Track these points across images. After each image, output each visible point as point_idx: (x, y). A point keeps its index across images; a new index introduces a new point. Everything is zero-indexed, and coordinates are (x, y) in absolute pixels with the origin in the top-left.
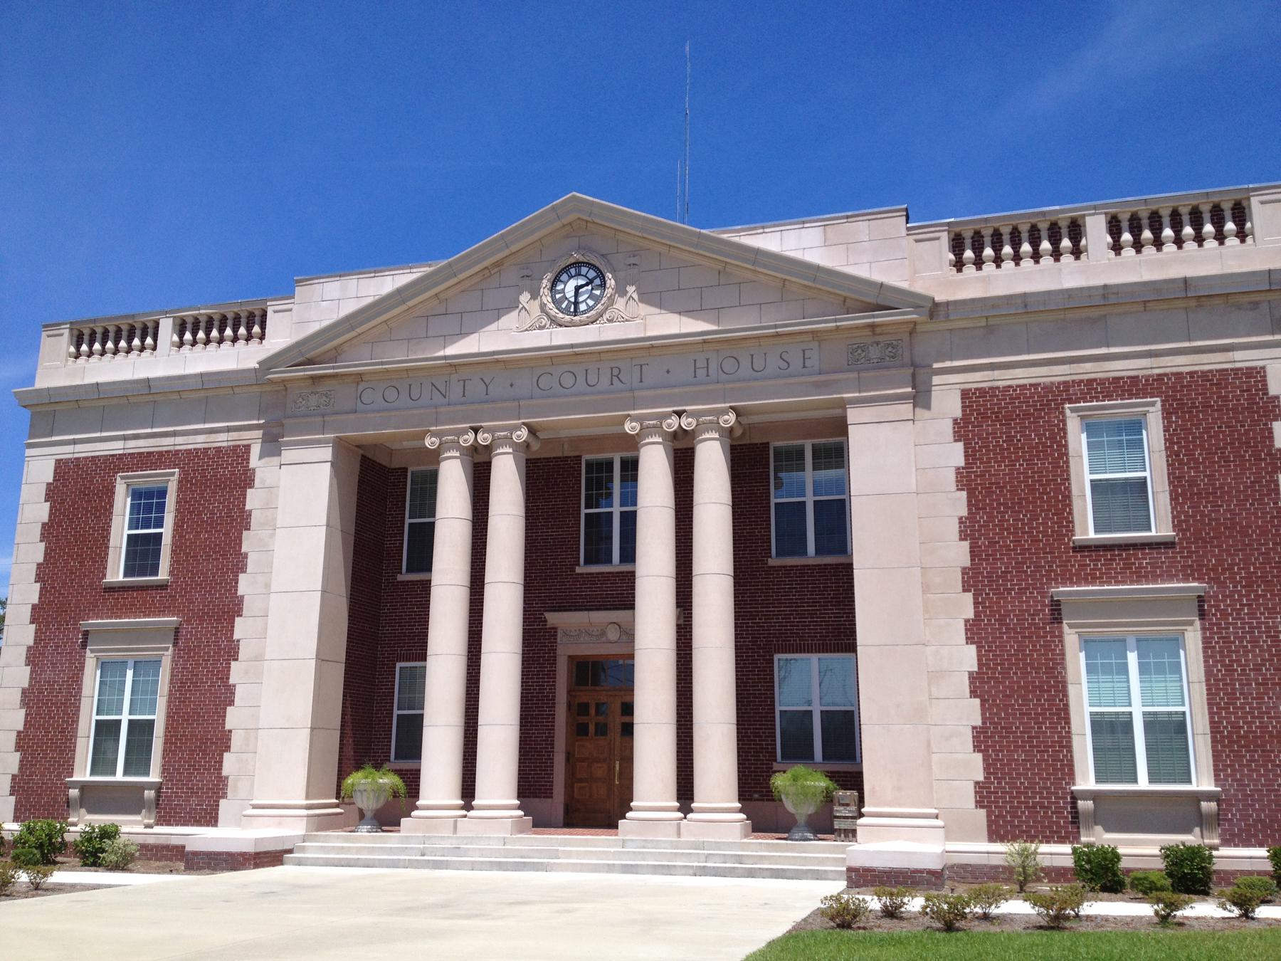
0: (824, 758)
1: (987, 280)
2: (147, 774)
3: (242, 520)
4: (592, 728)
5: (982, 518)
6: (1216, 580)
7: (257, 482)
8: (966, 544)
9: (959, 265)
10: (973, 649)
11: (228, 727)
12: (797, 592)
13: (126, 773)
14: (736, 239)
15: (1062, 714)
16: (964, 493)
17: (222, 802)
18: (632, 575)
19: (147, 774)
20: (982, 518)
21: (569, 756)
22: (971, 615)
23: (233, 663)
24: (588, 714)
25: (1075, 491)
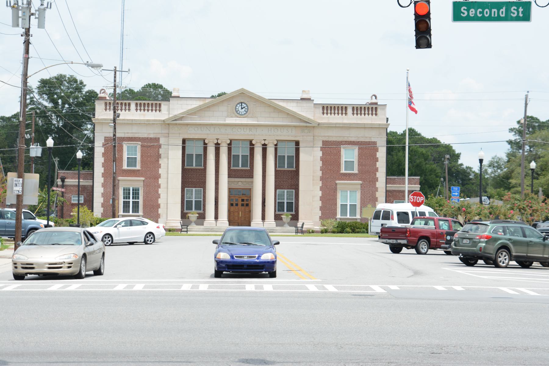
1: (329, 118)
2: (138, 212)
3: (159, 156)
5: (324, 167)
9: (323, 113)
12: (288, 178)
13: (133, 212)
15: (336, 204)
19: (138, 212)
20: (324, 167)
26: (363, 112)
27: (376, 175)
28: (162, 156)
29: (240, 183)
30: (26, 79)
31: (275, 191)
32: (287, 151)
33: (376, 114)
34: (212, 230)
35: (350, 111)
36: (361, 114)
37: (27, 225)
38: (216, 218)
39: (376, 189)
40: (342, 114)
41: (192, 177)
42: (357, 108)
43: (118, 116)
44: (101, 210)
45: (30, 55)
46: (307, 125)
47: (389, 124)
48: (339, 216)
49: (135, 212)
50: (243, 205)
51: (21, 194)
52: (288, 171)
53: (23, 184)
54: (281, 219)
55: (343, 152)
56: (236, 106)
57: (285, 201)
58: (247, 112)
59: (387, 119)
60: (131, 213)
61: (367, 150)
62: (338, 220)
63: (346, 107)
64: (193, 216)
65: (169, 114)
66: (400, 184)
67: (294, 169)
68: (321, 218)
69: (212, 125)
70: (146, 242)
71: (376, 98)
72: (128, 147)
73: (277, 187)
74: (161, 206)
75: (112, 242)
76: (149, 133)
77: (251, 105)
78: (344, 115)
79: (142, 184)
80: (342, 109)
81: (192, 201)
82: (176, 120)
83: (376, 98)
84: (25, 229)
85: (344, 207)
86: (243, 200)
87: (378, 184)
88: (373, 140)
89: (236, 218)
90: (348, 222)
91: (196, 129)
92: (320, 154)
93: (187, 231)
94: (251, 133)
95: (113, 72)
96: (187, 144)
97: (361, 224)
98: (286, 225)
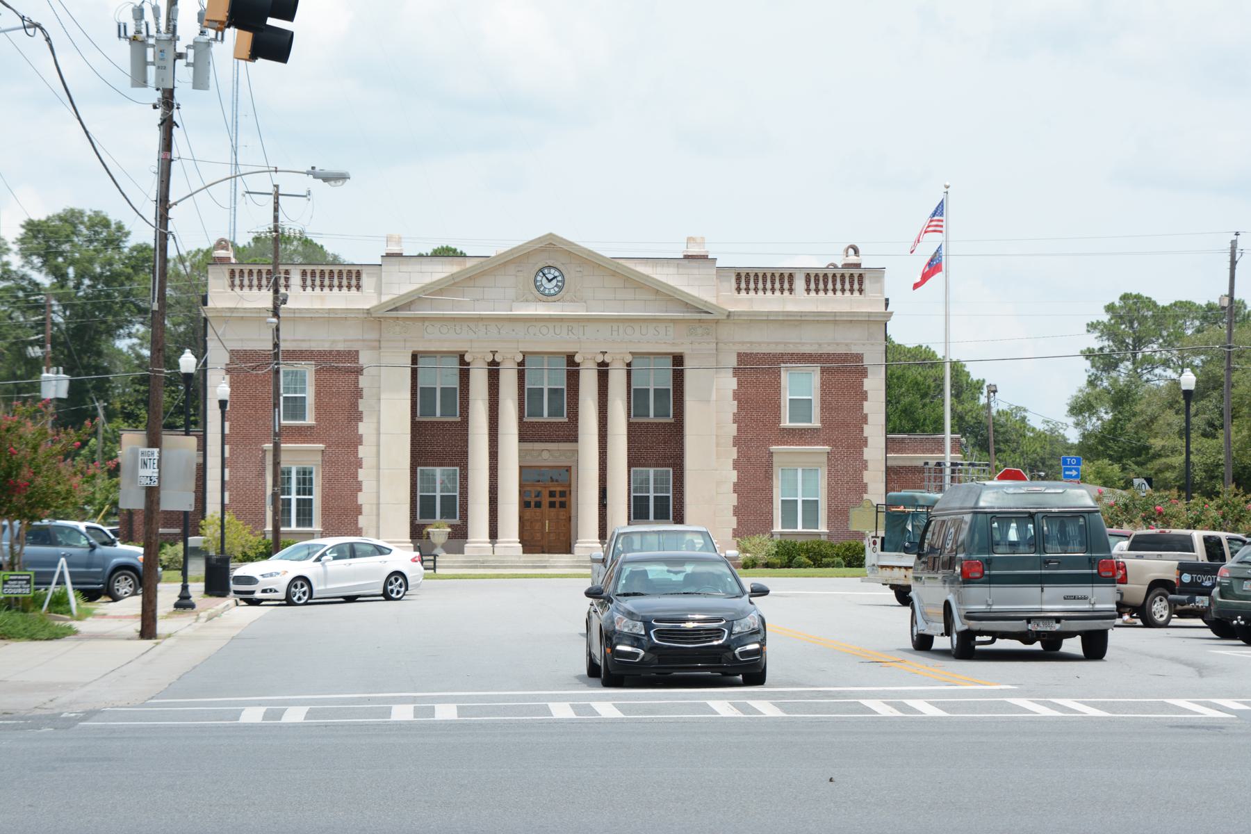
1: (751, 300)
2: (310, 525)
3: (358, 393)
9: (739, 290)
13: (298, 525)
19: (310, 525)
26: (830, 286)
27: (862, 431)
28: (365, 393)
29: (548, 454)
30: (167, 211)
31: (629, 471)
32: (657, 379)
33: (861, 291)
34: (483, 564)
35: (800, 284)
36: (826, 290)
37: (106, 558)
38: (493, 535)
39: (865, 465)
40: (782, 290)
41: (437, 441)
43: (284, 302)
45: (175, 154)
46: (701, 317)
47: (891, 313)
48: (778, 528)
49: (304, 526)
50: (552, 505)
51: (156, 484)
52: (657, 425)
53: (159, 461)
55: (785, 378)
56: (537, 274)
57: (652, 495)
58: (561, 288)
59: (887, 300)
61: (842, 373)
62: (777, 538)
64: (439, 531)
66: (915, 452)
67: (671, 420)
68: (736, 533)
69: (481, 319)
70: (387, 596)
71: (856, 252)
73: (634, 461)
74: (365, 509)
75: (310, 597)
76: (334, 342)
78: (786, 293)
79: (319, 458)
80: (781, 280)
82: (396, 309)
83: (856, 252)
84: (105, 569)
86: (552, 494)
87: (868, 453)
88: (855, 350)
90: (800, 540)
92: (732, 383)
93: (434, 568)
95: (271, 198)
96: (422, 362)
97: (832, 546)
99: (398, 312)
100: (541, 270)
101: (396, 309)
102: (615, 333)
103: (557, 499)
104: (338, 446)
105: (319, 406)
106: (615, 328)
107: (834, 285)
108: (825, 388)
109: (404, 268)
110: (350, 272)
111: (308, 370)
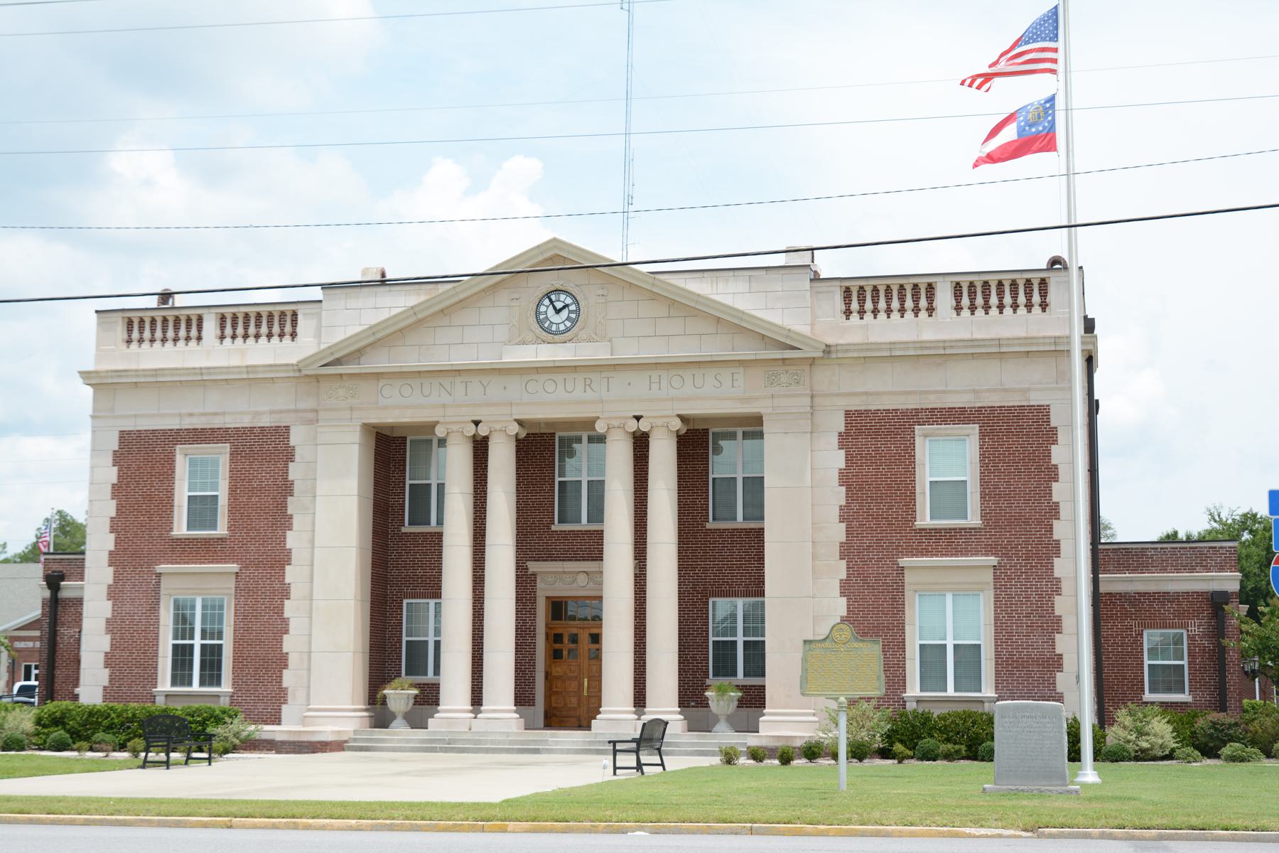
0: (745, 675)
1: (866, 327)
2: (219, 684)
3: (287, 489)
4: (565, 653)
5: (855, 506)
6: (1006, 555)
7: (297, 458)
8: (844, 525)
9: (848, 313)
10: (843, 602)
11: (285, 650)
12: (722, 557)
13: (202, 683)
14: (682, 285)
16: (844, 489)
17: (284, 707)
18: (600, 534)
19: (219, 684)
20: (855, 506)
21: (547, 675)
22: (844, 577)
23: (286, 602)
24: (562, 642)
25: (918, 491)
26: (994, 300)
28: (297, 488)
33: (1044, 306)
35: (944, 298)
38: (477, 699)
39: (1056, 587)
40: (916, 311)
41: (400, 563)
42: (972, 285)
44: (103, 676)
46: (785, 357)
54: (704, 703)
56: (540, 303)
57: (740, 639)
58: (574, 322)
60: (196, 687)
63: (930, 287)
65: (319, 344)
66: (1164, 570)
72: (193, 463)
74: (292, 660)
76: (257, 414)
77: (590, 293)
78: (923, 314)
79: (232, 585)
80: (915, 293)
81: (426, 642)
82: (337, 362)
85: (932, 656)
88: (1036, 399)
89: (574, 700)
91: (407, 391)
92: (838, 459)
94: (590, 395)
98: (722, 726)
99: (338, 367)
100: (548, 295)
101: (337, 362)
102: (655, 386)
103: (566, 645)
104: (257, 567)
105: (232, 509)
106: (655, 379)
107: (1001, 299)
108: (989, 461)
109: (353, 303)
110: (283, 314)
111: (221, 455)
